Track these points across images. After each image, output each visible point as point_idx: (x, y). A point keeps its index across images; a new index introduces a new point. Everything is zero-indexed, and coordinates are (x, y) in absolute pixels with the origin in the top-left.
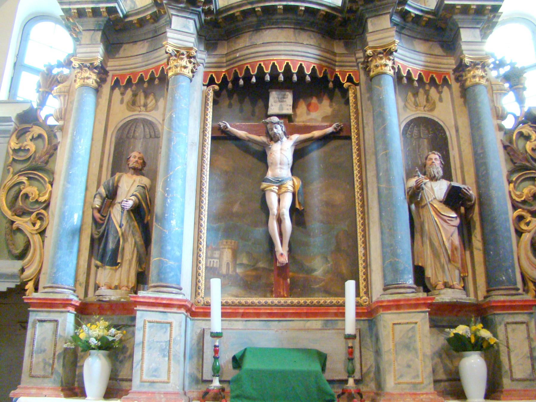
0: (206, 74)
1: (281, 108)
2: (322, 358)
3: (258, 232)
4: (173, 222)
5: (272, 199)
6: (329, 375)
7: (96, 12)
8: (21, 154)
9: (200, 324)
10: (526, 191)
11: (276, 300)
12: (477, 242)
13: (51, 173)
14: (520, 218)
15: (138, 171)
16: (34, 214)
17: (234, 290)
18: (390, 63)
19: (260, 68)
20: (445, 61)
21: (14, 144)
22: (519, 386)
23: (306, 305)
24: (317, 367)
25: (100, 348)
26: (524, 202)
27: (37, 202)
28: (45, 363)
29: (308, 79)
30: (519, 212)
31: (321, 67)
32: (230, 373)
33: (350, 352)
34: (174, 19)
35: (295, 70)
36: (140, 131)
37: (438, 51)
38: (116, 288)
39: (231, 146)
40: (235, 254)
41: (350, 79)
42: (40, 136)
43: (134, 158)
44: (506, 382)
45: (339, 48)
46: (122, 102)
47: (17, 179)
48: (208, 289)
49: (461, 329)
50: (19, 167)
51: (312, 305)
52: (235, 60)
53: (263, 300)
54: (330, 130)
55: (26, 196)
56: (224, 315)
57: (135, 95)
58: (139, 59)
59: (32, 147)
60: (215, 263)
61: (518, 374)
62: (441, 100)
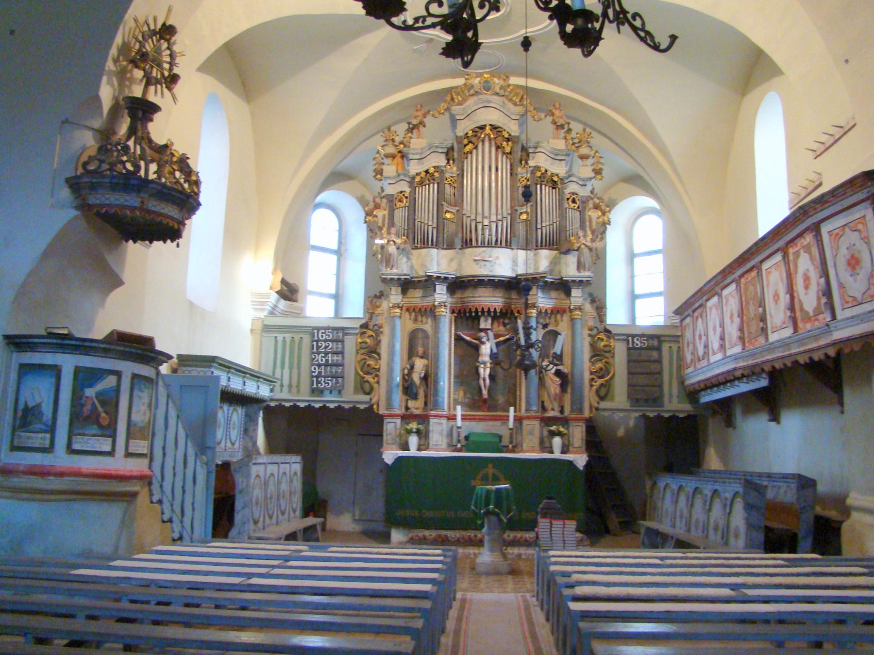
0: (451, 307)
1: (486, 326)
2: (500, 437)
3: (474, 383)
4: (442, 383)
5: (481, 371)
6: (503, 444)
7: (399, 279)
8: (363, 344)
9: (452, 423)
10: (597, 366)
11: (482, 413)
12: (569, 390)
13: (379, 355)
14: (592, 379)
15: (422, 357)
16: (374, 375)
17: (465, 409)
18: (534, 311)
19: (476, 309)
20: (565, 301)
21: (360, 340)
22: (576, 450)
23: (494, 416)
24: (497, 440)
25: (415, 432)
26: (596, 372)
27: (374, 368)
28: (392, 438)
29: (498, 314)
30: (592, 376)
31: (504, 306)
32: (464, 442)
33: (511, 436)
34: (437, 287)
35: (492, 310)
36: (420, 335)
37: (563, 296)
38: (417, 409)
39: (462, 343)
40: (465, 394)
41: (518, 312)
42: (372, 336)
43: (420, 350)
44: (571, 449)
45: (514, 295)
46: (410, 319)
47: (363, 357)
48: (455, 409)
49: (553, 428)
50: (363, 351)
51: (497, 416)
52: (464, 302)
53: (477, 413)
54: (507, 337)
55: (369, 365)
56: (462, 419)
57: (416, 316)
58: (418, 299)
59: (368, 340)
60: (456, 397)
61: (576, 445)
62: (562, 321)
